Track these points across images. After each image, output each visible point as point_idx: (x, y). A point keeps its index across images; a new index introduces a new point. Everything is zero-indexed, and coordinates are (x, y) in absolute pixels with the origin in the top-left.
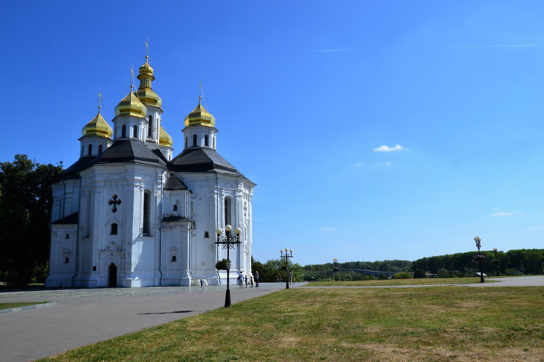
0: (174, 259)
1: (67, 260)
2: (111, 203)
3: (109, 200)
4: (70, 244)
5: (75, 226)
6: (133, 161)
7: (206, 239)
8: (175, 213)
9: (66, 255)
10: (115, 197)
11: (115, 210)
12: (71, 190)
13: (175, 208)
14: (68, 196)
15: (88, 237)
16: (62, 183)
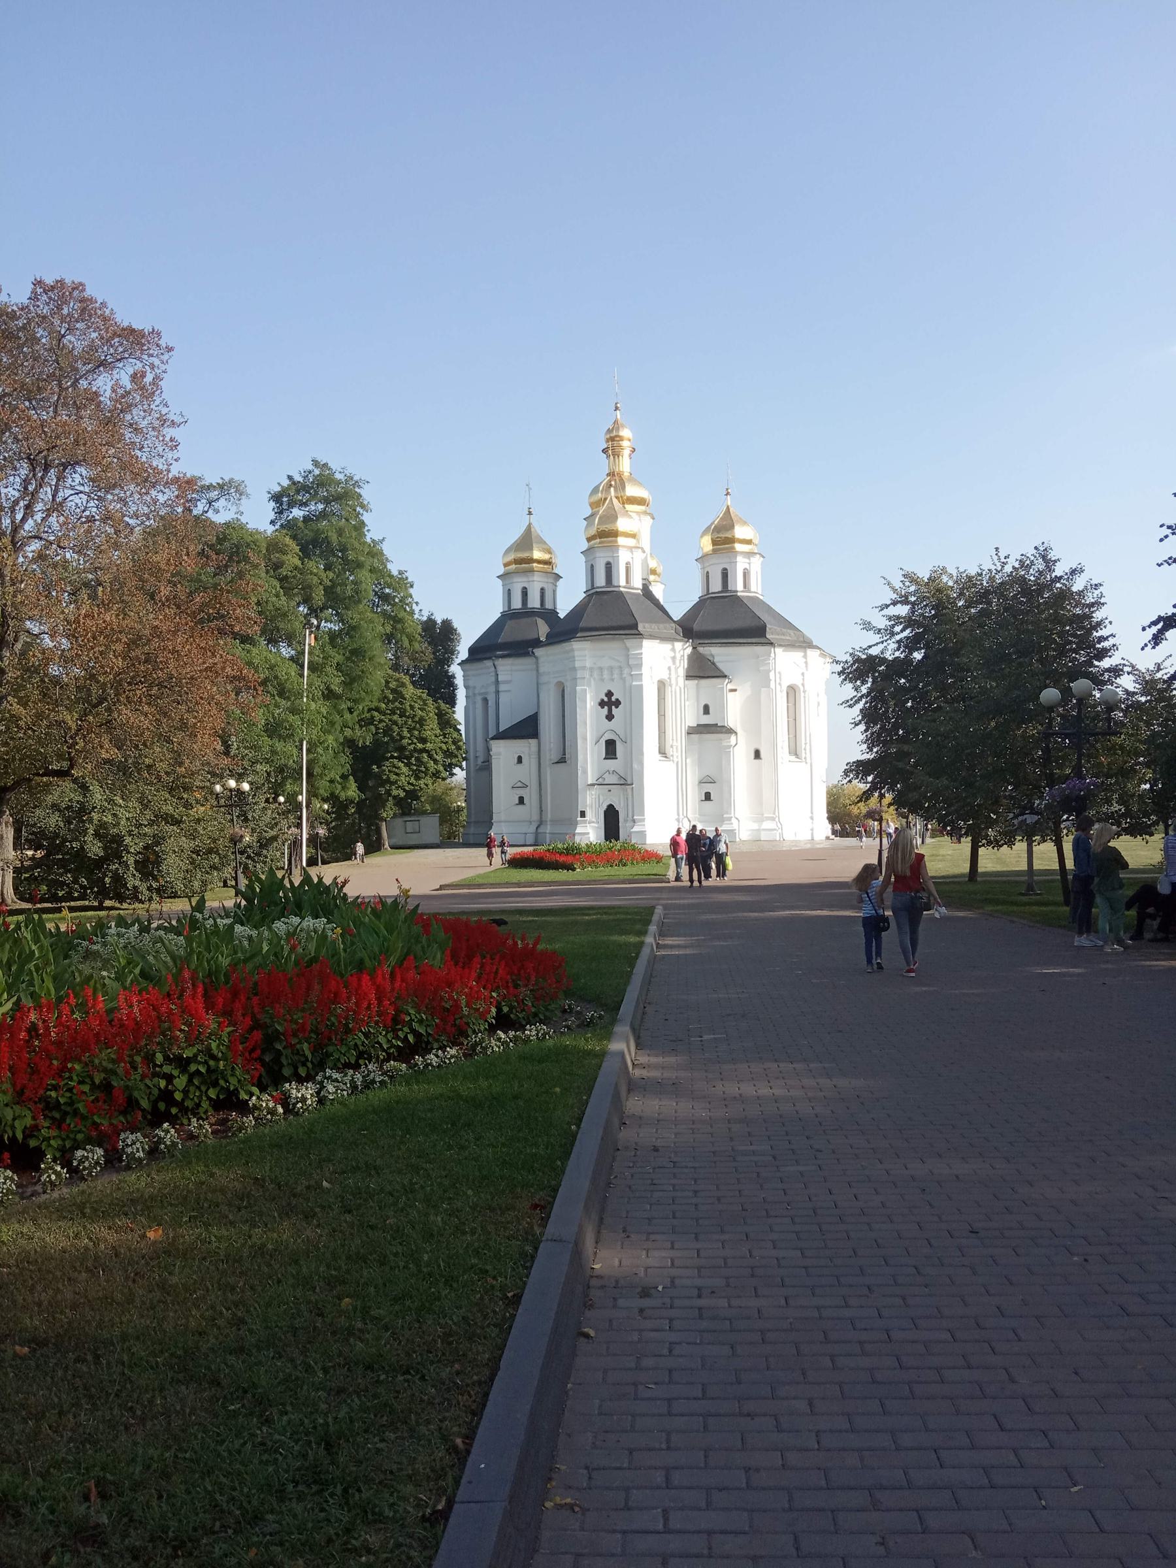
0: (708, 797)
1: (521, 801)
2: (602, 704)
3: (599, 701)
4: (527, 772)
5: (533, 742)
6: (637, 632)
7: (757, 761)
8: (706, 720)
9: (521, 792)
10: (609, 694)
11: (610, 717)
12: (507, 678)
13: (706, 710)
14: (502, 687)
15: (562, 761)
16: (489, 663)
